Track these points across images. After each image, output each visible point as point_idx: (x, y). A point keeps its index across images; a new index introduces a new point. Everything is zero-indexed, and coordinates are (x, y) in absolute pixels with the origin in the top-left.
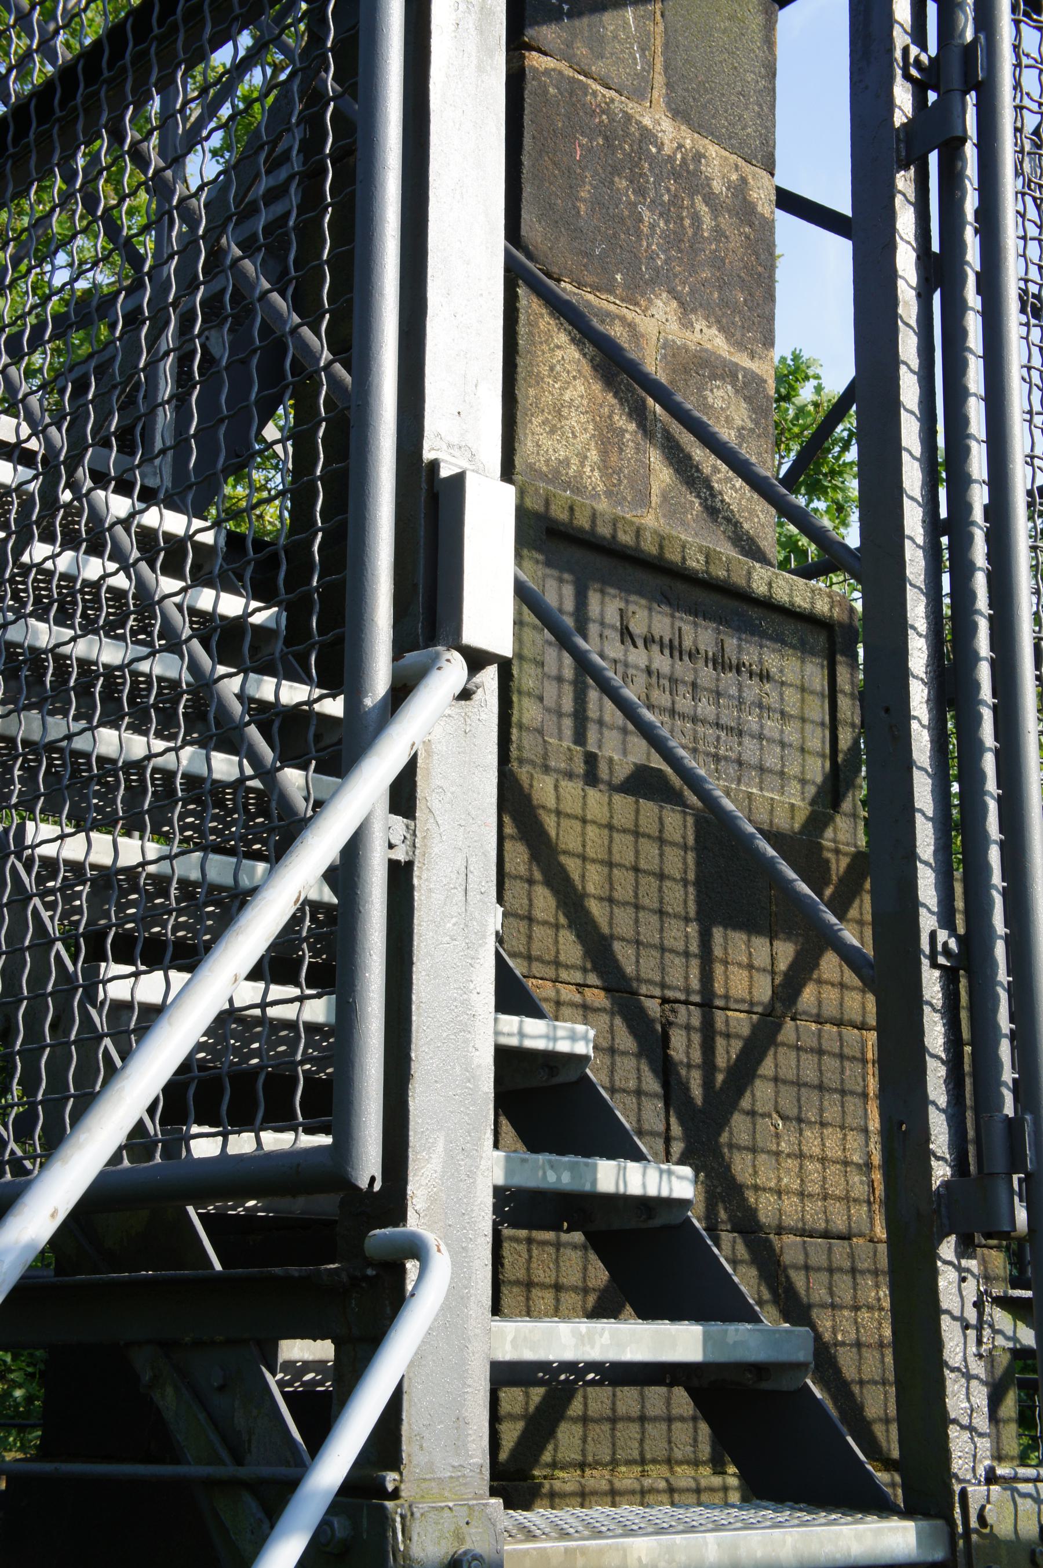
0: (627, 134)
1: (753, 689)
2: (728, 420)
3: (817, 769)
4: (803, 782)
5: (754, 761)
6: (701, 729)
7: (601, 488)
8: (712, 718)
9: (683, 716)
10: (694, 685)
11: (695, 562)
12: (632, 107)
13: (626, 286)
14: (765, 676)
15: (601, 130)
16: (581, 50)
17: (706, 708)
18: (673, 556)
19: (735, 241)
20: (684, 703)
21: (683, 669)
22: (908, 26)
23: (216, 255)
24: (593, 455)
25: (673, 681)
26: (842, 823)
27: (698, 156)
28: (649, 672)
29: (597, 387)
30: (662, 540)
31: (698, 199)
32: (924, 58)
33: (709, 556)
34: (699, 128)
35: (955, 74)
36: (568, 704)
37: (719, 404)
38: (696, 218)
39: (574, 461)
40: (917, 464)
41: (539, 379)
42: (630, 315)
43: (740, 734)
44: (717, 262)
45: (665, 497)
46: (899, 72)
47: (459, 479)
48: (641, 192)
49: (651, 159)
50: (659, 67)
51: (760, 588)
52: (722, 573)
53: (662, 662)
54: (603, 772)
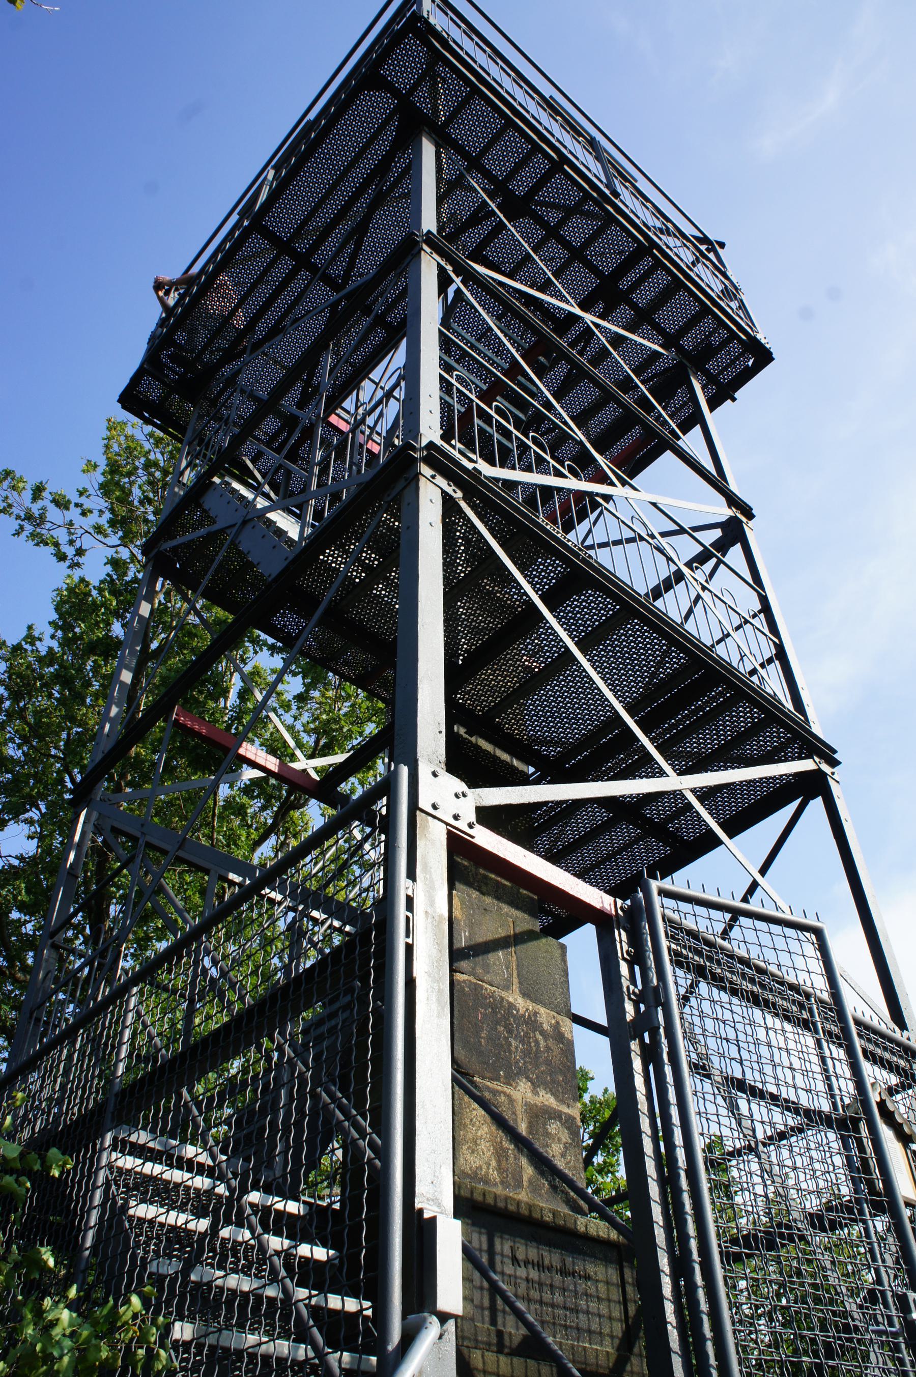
0: (502, 1006)
1: (582, 1285)
2: (559, 1139)
3: (618, 1329)
4: (612, 1337)
5: (585, 1327)
6: (556, 1311)
7: (498, 1180)
8: (562, 1304)
9: (547, 1304)
10: (551, 1286)
11: (548, 1217)
12: (504, 994)
13: (506, 1077)
14: (587, 1278)
15: (490, 1005)
16: (479, 971)
17: (558, 1298)
18: (536, 1215)
19: (556, 1052)
20: (547, 1296)
21: (545, 1277)
22: (628, 977)
23: (315, 1097)
24: (494, 1163)
25: (541, 1284)
26: (634, 1360)
27: (536, 1014)
28: (527, 1280)
29: (494, 1128)
30: (530, 1207)
31: (537, 1033)
32: (636, 991)
33: (555, 1213)
34: (535, 1001)
35: (651, 997)
36: (486, 1303)
37: (554, 1132)
38: (537, 1042)
39: (484, 1167)
40: (655, 1183)
41: (465, 1125)
42: (508, 1091)
43: (577, 1312)
44: (548, 1063)
45: (530, 1182)
46: (626, 998)
47: (433, 1219)
48: (510, 1032)
49: (514, 1016)
50: (515, 975)
51: (581, 1228)
52: (562, 1222)
53: (534, 1274)
54: (507, 1342)
